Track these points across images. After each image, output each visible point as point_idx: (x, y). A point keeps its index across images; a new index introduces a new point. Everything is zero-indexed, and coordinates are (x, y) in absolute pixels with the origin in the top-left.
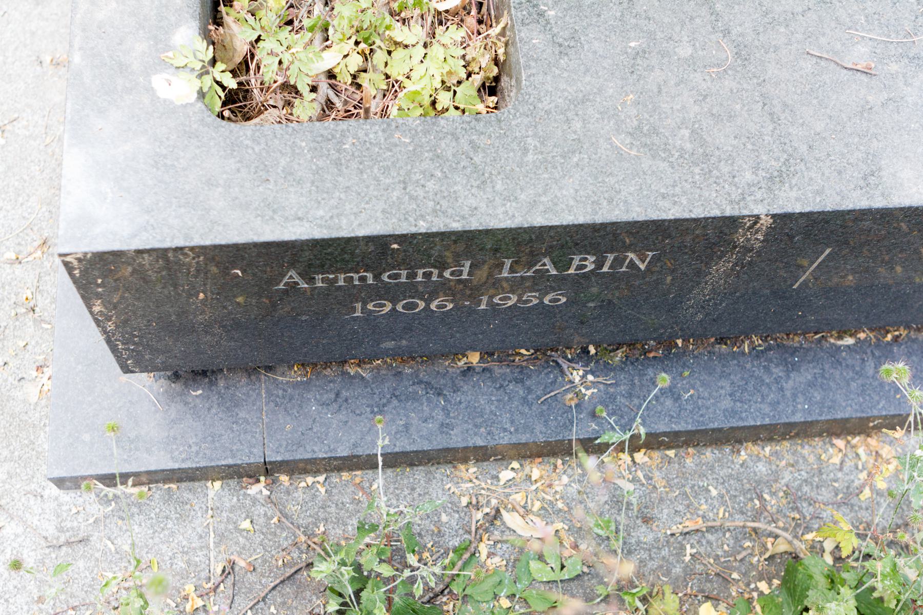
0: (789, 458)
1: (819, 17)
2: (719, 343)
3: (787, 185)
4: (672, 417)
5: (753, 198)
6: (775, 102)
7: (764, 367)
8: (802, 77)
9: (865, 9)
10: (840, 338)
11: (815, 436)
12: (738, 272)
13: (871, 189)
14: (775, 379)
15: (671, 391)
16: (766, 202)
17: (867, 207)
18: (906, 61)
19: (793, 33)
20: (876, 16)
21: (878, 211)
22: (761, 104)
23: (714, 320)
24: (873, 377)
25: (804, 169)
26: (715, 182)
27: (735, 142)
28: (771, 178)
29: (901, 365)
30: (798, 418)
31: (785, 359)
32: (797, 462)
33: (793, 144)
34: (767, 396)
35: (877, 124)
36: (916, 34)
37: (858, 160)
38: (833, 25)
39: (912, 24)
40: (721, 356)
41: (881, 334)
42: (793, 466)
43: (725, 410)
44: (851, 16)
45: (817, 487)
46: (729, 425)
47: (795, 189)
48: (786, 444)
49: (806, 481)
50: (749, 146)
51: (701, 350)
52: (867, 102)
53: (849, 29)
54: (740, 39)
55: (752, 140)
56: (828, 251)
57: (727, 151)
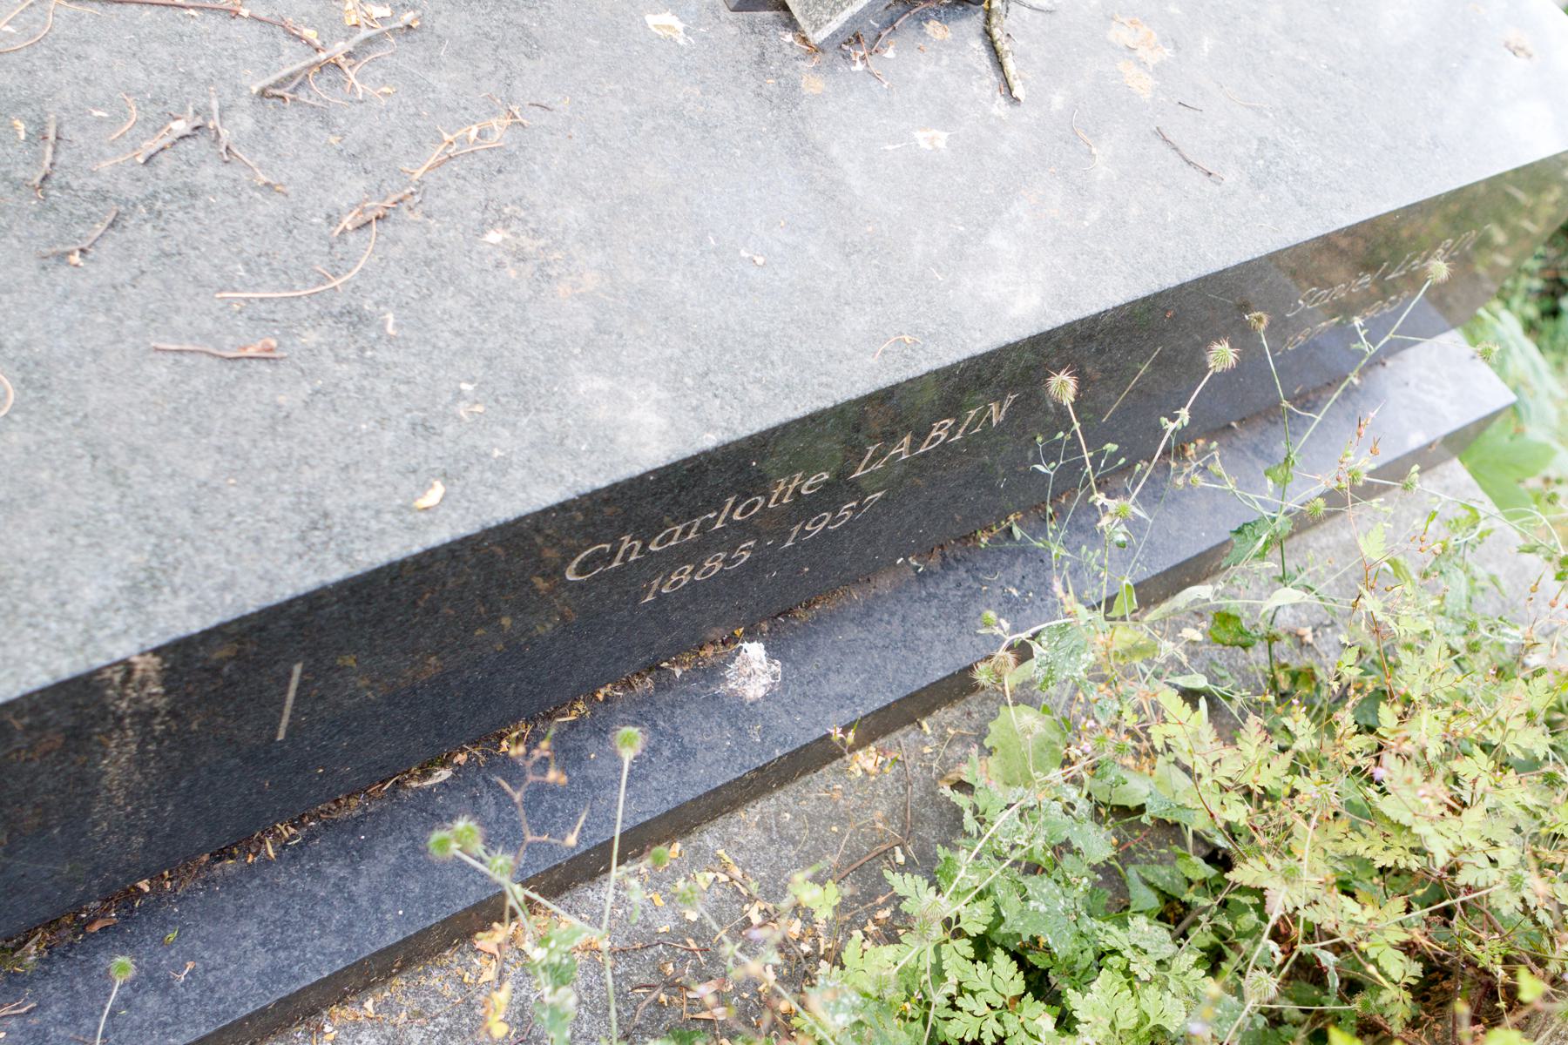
0: (411, 1003)
1: (164, 282)
2: (220, 860)
3: (167, 590)
4: (166, 1024)
5: (107, 631)
6: (114, 449)
7: (311, 871)
8: (153, 392)
9: (240, 252)
10: (426, 774)
11: (442, 950)
12: (157, 753)
13: (317, 552)
14: (335, 885)
15: (151, 979)
16: (133, 632)
17: (318, 586)
18: (330, 321)
19: (120, 320)
20: (263, 259)
21: (342, 585)
22: (88, 459)
23: (169, 836)
24: (497, 821)
25: (191, 552)
26: (30, 625)
27: (52, 541)
28: (135, 588)
29: (461, 824)
30: (393, 936)
31: (344, 844)
32: (426, 1005)
33: (163, 514)
34: (329, 919)
35: (304, 440)
36: (336, 275)
37: (285, 509)
38: (191, 290)
39: (326, 259)
40: (228, 882)
41: (492, 745)
42: (420, 1015)
43: (262, 973)
44: (218, 268)
45: (471, 1032)
46: (274, 998)
47: (183, 592)
48: (398, 981)
49: (449, 1031)
50: (81, 541)
51: (189, 884)
52: (279, 407)
53: (221, 290)
54: (25, 353)
55: (85, 528)
56: (297, 669)
57: (41, 561)
